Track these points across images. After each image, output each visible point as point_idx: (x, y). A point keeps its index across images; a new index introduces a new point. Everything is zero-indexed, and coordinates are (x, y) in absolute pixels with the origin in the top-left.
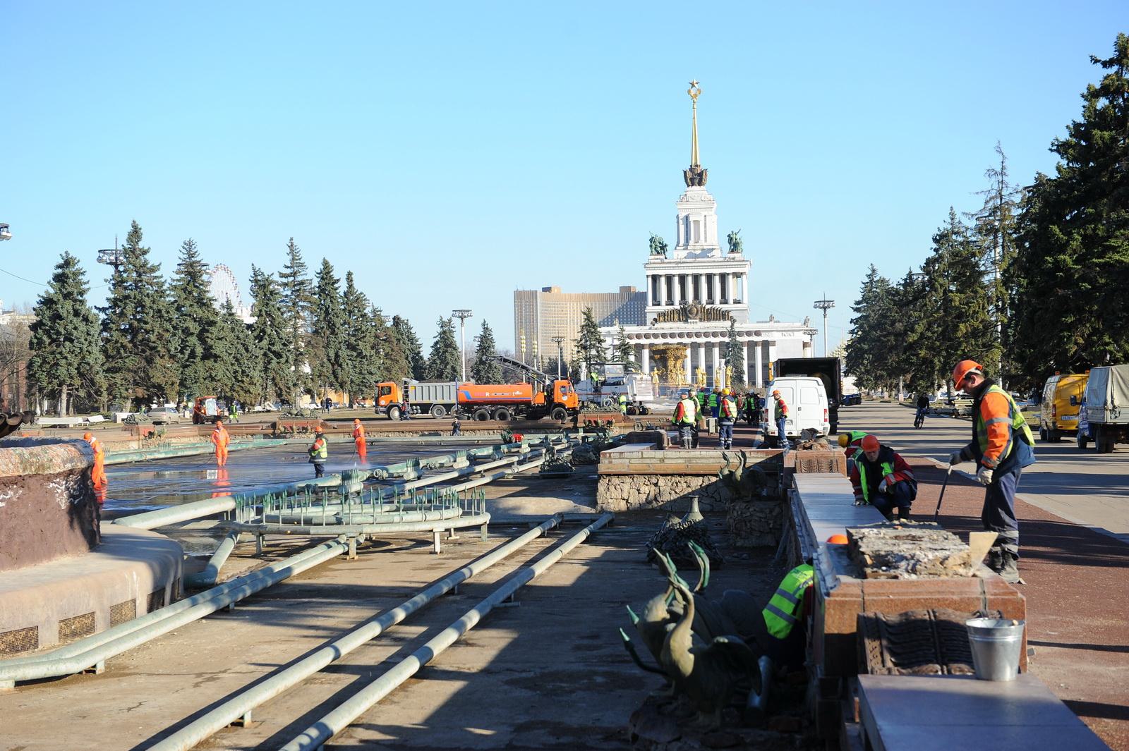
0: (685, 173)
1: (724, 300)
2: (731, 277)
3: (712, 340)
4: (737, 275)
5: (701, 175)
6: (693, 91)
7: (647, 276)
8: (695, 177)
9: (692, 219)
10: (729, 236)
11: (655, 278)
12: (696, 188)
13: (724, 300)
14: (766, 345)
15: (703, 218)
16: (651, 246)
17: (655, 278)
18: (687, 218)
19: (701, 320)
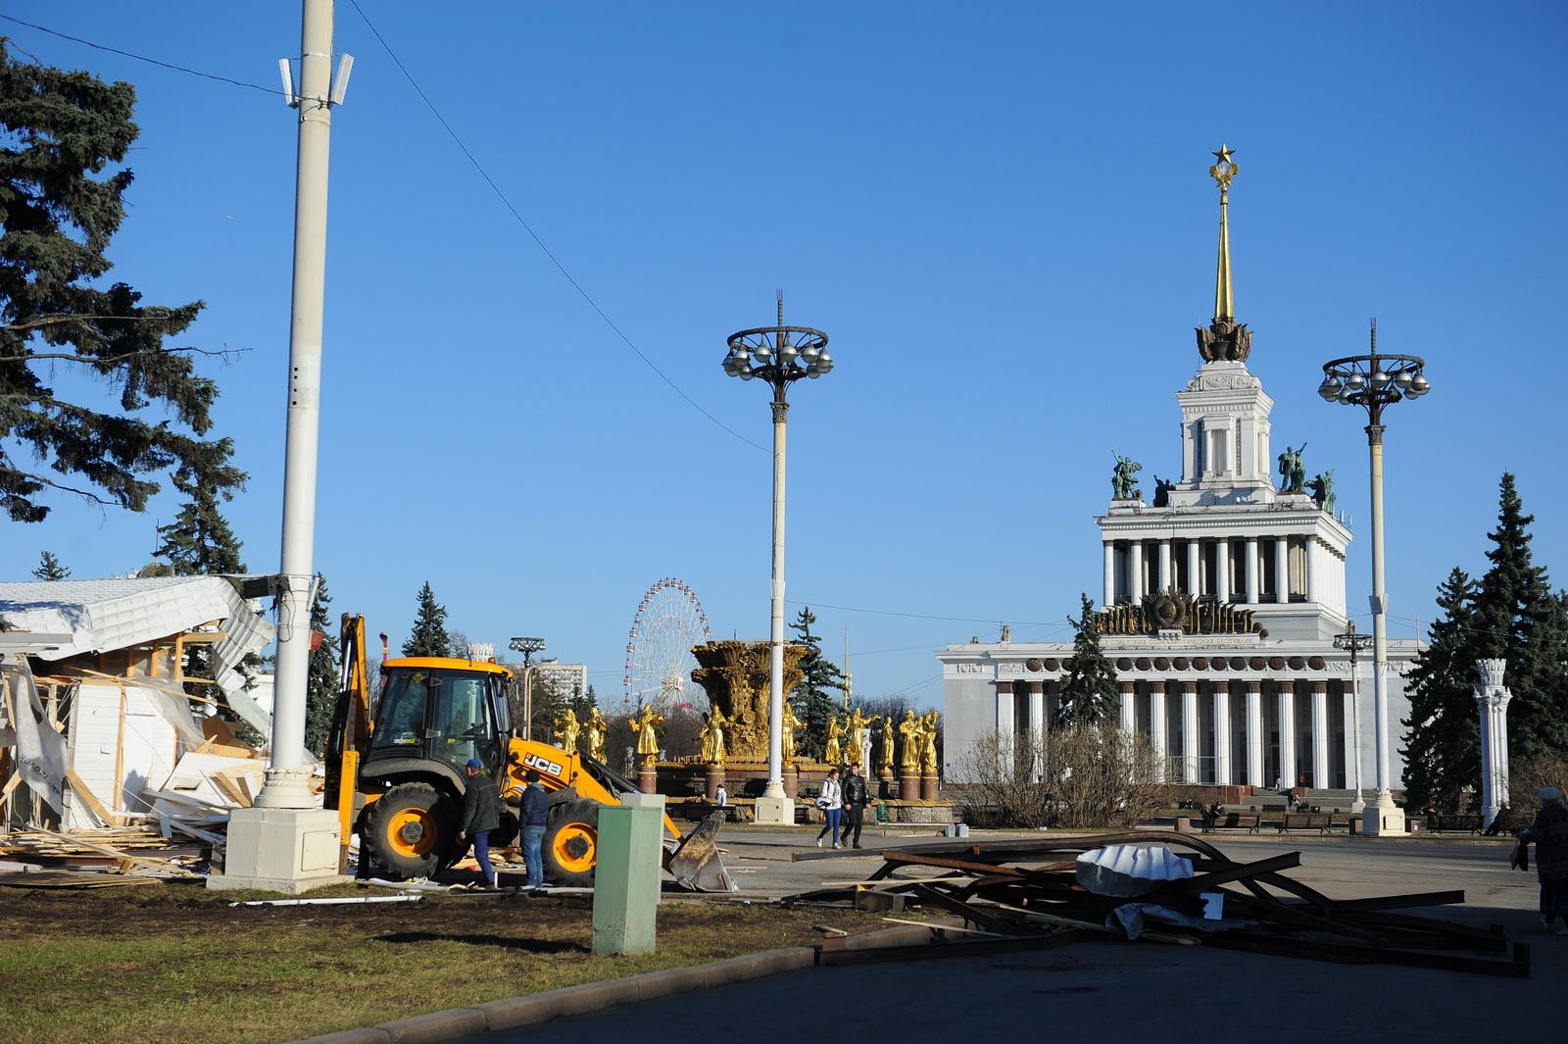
0: (1199, 333)
1: (1270, 595)
2: (1283, 546)
3: (1211, 675)
4: (1300, 541)
5: (1232, 337)
6: (1222, 170)
7: (1105, 543)
8: (1222, 342)
9: (1208, 426)
10: (1281, 458)
11: (1123, 548)
12: (1223, 365)
13: (1270, 595)
14: (1337, 690)
15: (1233, 425)
16: (1115, 481)
17: (1123, 548)
18: (1200, 424)
19: (1187, 631)
